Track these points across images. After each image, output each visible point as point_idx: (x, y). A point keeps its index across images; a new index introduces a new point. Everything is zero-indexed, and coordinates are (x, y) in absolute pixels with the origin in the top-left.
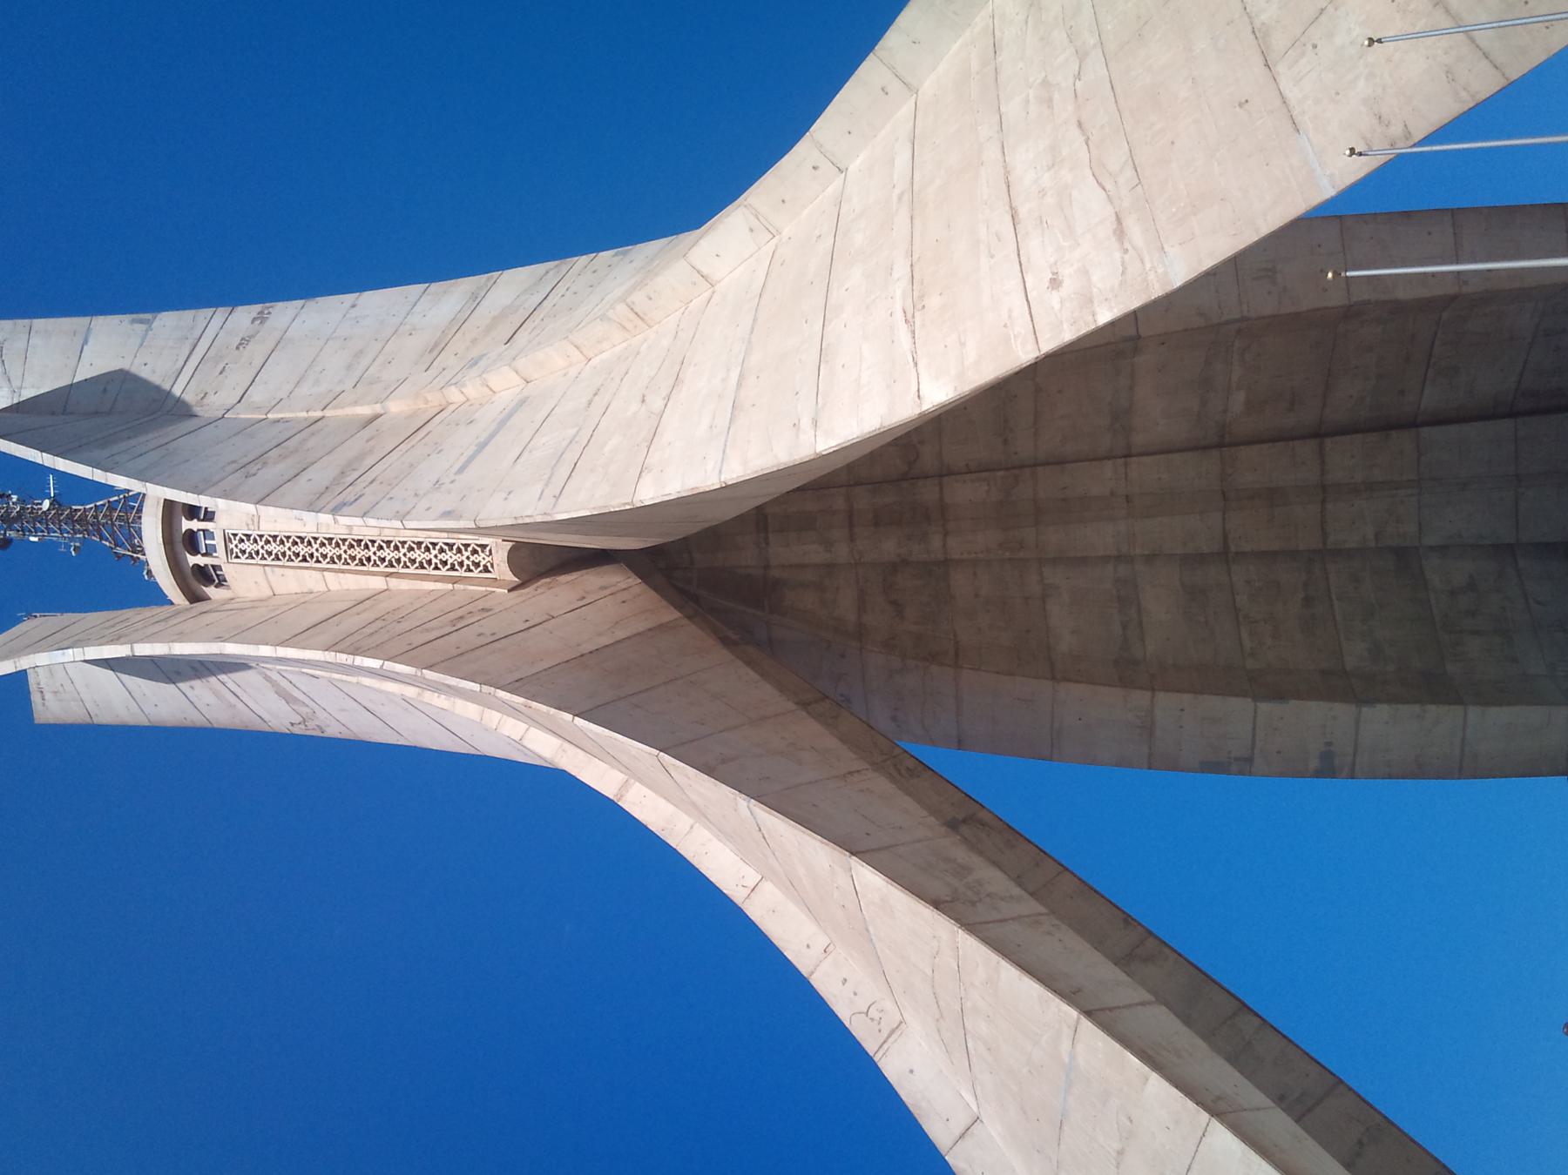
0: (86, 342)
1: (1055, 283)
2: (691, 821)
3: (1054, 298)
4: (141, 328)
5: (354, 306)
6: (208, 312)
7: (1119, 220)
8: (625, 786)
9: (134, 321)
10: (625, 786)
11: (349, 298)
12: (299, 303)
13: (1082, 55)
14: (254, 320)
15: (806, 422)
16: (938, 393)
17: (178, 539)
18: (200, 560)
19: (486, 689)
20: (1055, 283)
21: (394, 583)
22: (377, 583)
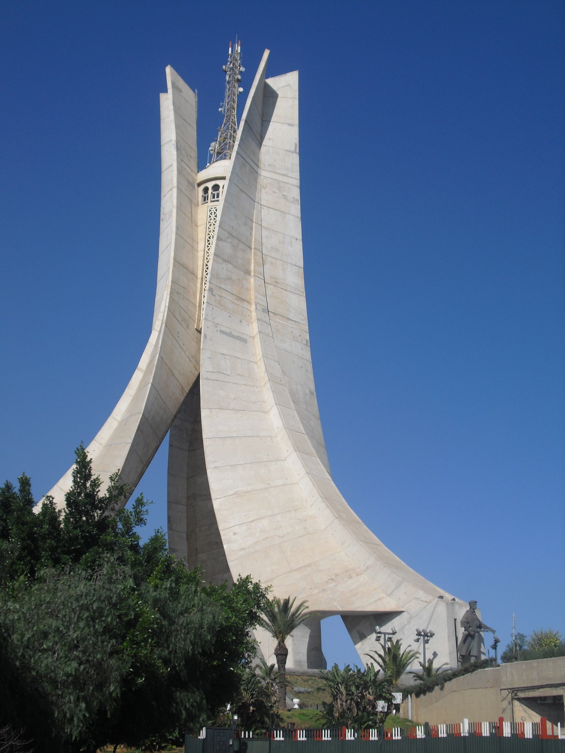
0: (289, 125)
1: (235, 534)
2: (133, 395)
3: (231, 534)
4: (293, 149)
5: (297, 239)
6: (298, 177)
7: (244, 549)
8: (141, 370)
9: (296, 144)
10: (141, 370)
11: (300, 237)
12: (299, 215)
13: (282, 537)
14: (294, 198)
15: (216, 464)
16: (216, 504)
17: (217, 182)
18: (210, 191)
19: (159, 349)
20: (235, 534)
21: (199, 281)
22: (199, 276)
